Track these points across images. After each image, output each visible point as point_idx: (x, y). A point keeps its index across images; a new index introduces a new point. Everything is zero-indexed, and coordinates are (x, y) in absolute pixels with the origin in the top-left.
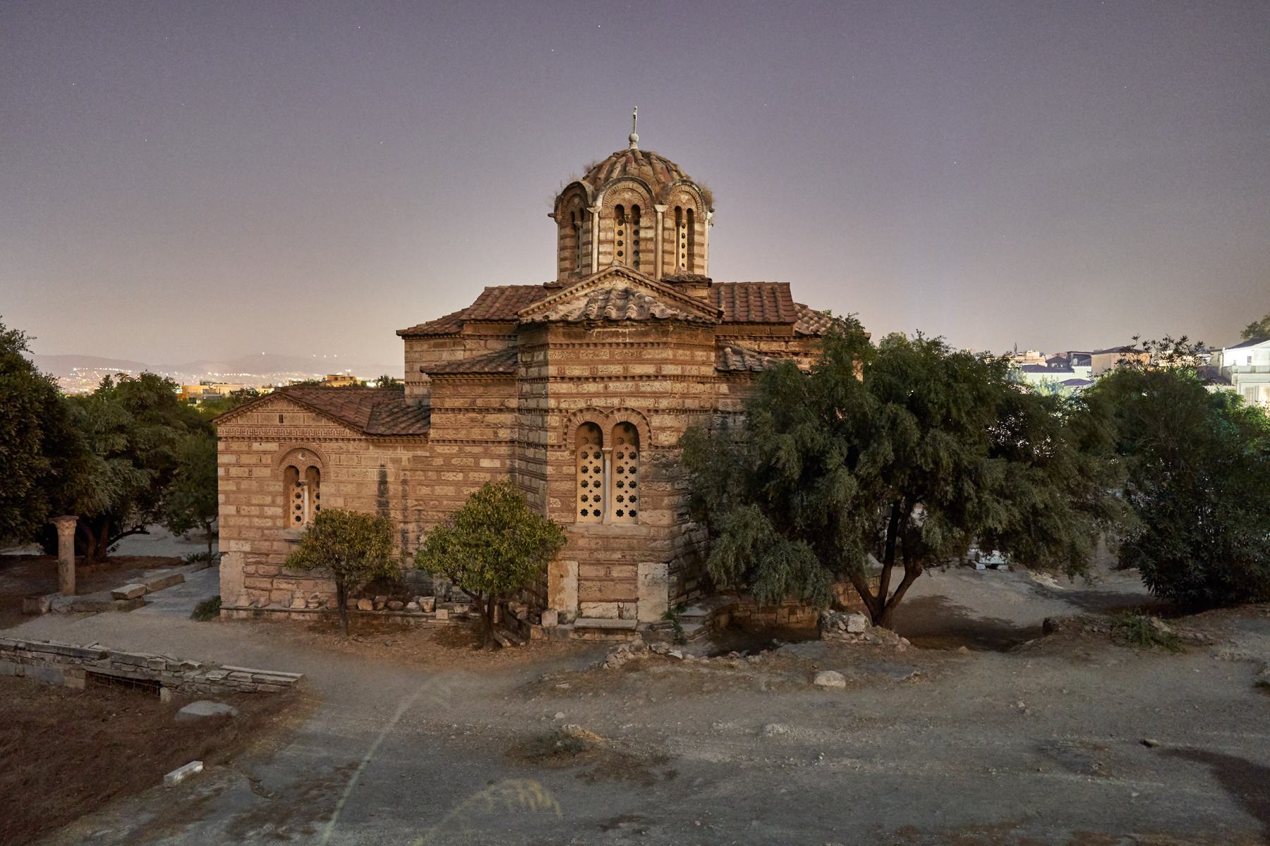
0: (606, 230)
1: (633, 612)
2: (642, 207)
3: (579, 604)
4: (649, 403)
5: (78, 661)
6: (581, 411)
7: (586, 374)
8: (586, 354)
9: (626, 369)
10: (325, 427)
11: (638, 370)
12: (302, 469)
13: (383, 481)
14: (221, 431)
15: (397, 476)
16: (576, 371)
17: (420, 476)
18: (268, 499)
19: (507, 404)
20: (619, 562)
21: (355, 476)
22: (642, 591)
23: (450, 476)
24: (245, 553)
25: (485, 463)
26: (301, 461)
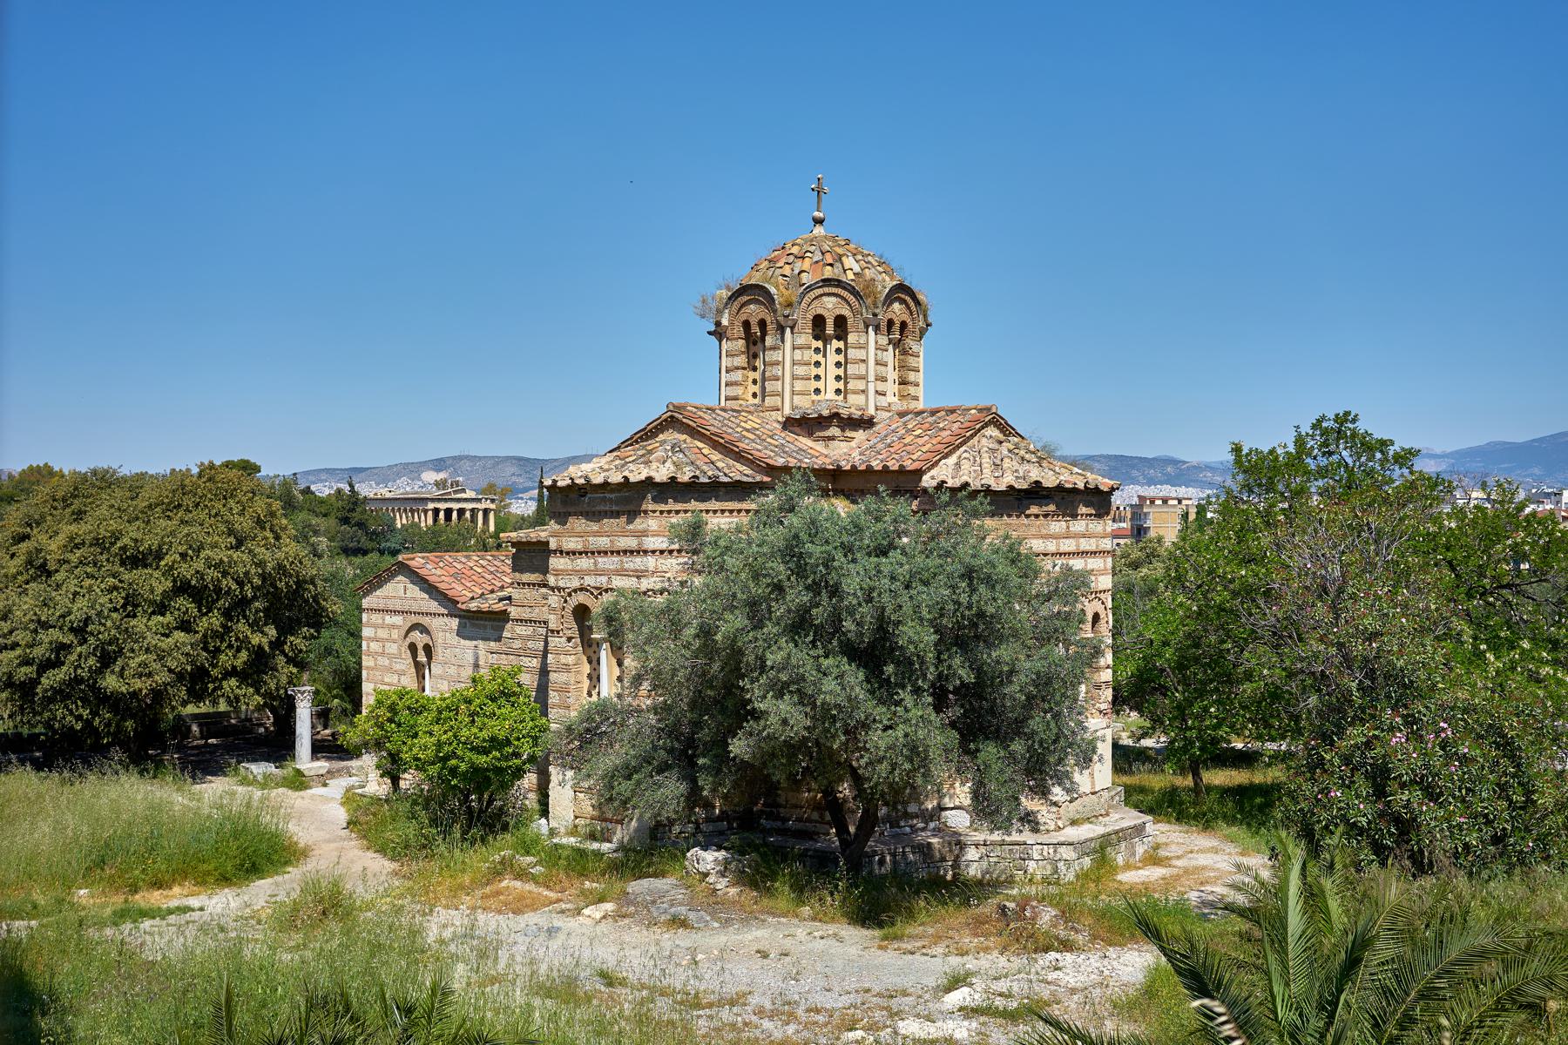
2: (768, 322)
6: (575, 591)
7: (580, 547)
12: (420, 646)
14: (365, 603)
16: (572, 544)
26: (418, 638)
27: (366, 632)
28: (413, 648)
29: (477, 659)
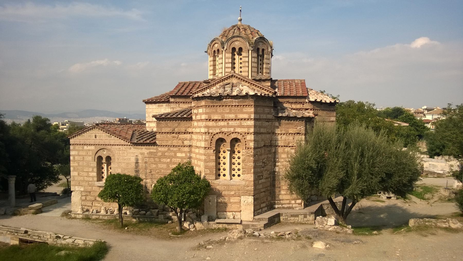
0: (228, 58)
1: (239, 216)
3: (217, 213)
4: (245, 130)
5: (16, 234)
6: (217, 133)
7: (220, 118)
8: (220, 110)
10: (114, 140)
11: (241, 116)
13: (137, 163)
14: (72, 141)
15: (143, 160)
16: (216, 117)
17: (152, 160)
18: (91, 170)
19: (187, 130)
20: (233, 196)
21: (126, 159)
22: (243, 208)
23: (164, 160)
24: (82, 191)
25: (179, 155)
26: (104, 154)
27: (72, 153)
28: (100, 158)
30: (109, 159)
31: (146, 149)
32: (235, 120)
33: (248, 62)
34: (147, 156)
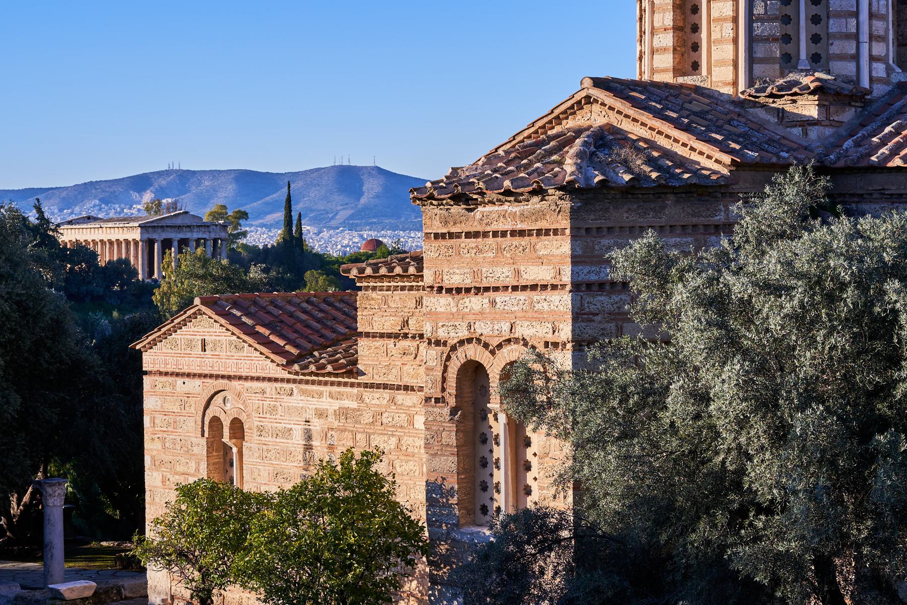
6: (461, 343)
7: (468, 282)
9: (518, 273)
13: (308, 448)
14: (149, 361)
27: (150, 403)
29: (309, 437)
30: (238, 427)
31: (331, 396)
32: (515, 288)
33: (735, 20)
34: (336, 424)
